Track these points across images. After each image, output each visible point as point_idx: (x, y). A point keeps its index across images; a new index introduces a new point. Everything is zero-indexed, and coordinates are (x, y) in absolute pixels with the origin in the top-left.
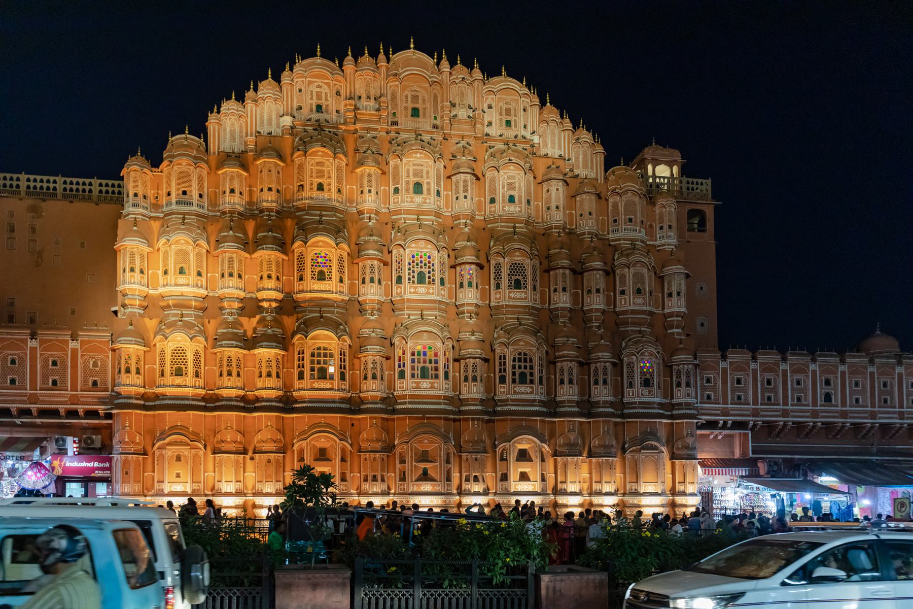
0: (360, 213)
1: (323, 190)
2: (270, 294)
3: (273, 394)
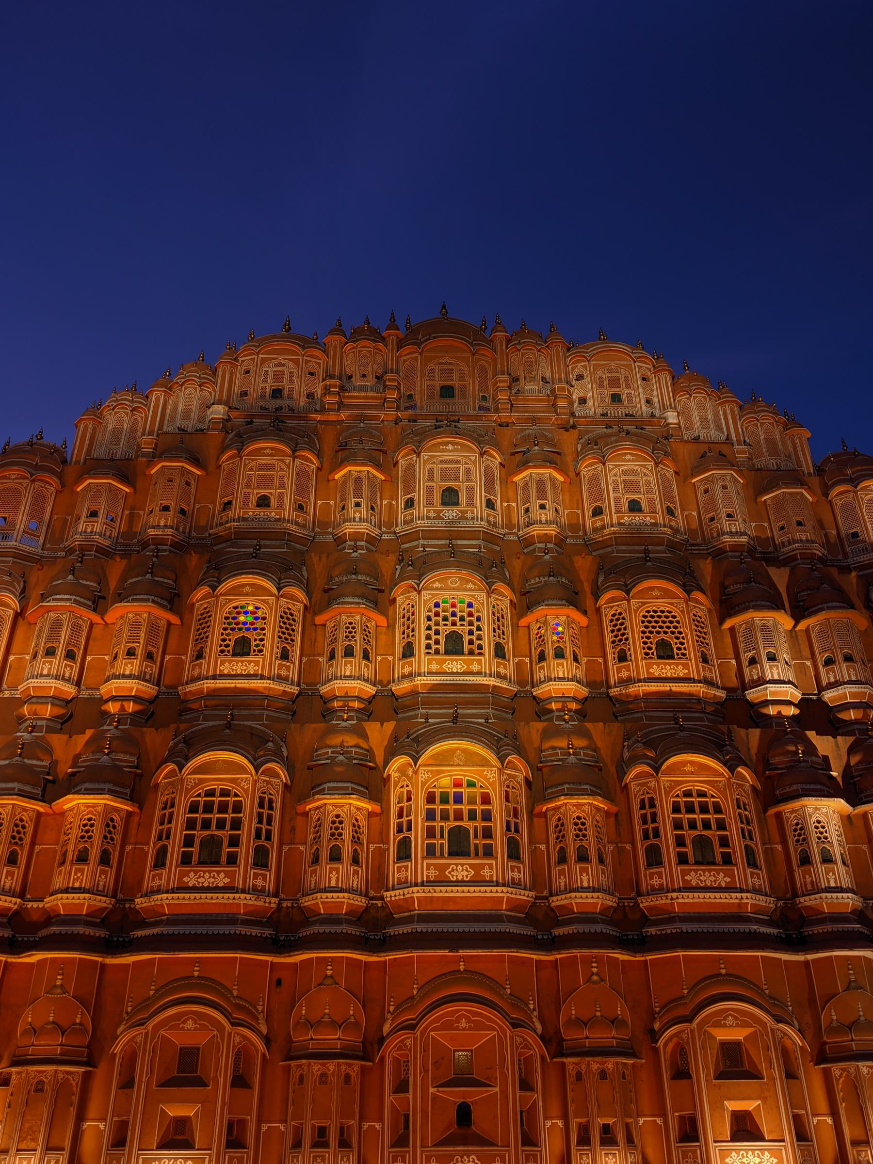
0: (340, 540)
1: (268, 505)
2: (124, 682)
3: (83, 902)
